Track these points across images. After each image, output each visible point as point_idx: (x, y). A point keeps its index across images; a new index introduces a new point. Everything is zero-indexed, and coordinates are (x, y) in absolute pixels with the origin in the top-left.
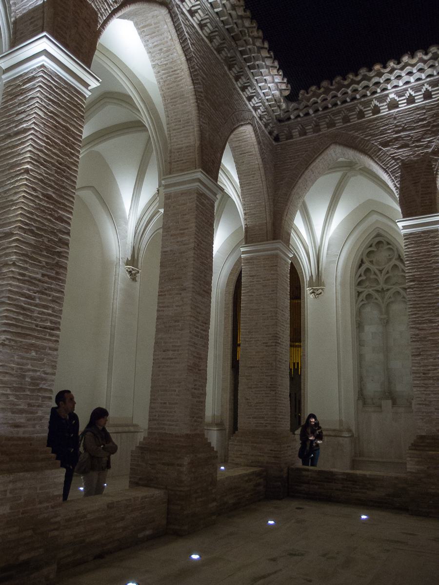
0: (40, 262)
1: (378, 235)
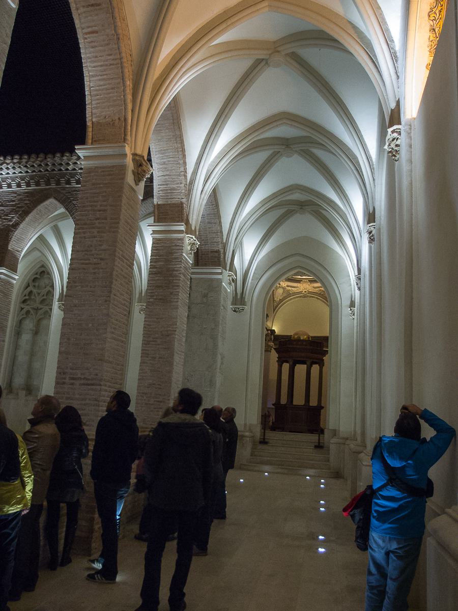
1: (43, 266)
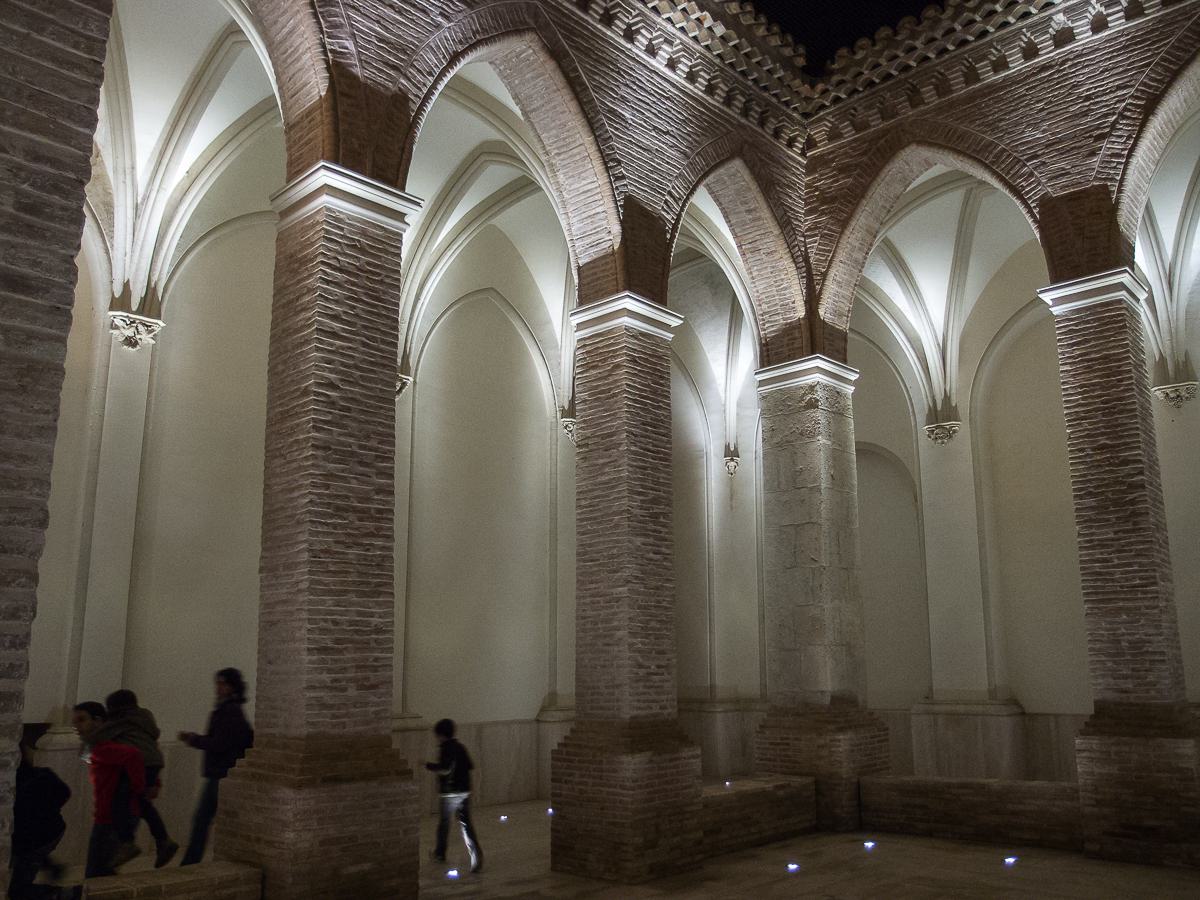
0: (1108, 520)
